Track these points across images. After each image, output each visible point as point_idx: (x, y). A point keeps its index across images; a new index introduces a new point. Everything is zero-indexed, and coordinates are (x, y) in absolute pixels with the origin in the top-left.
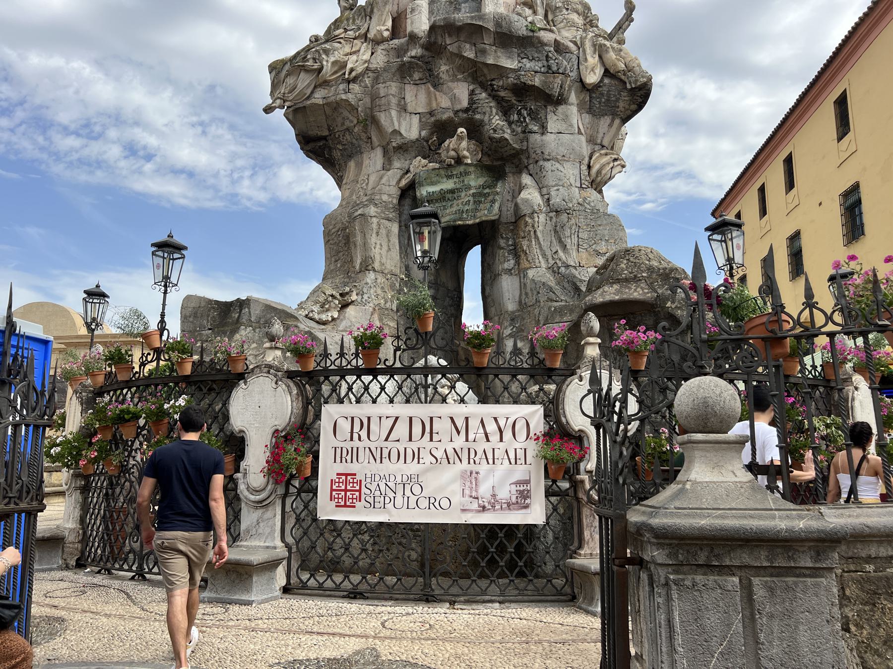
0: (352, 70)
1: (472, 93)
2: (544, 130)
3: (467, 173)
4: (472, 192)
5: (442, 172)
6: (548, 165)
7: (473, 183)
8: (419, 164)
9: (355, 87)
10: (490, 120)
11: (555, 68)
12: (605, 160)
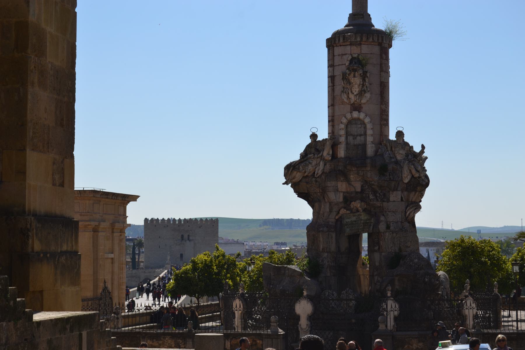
0: (317, 174)
1: (362, 186)
2: (388, 201)
3: (361, 215)
4: (362, 222)
5: (351, 214)
6: (389, 214)
7: (363, 218)
8: (343, 211)
9: (318, 179)
10: (369, 196)
11: (392, 179)
12: (411, 210)
